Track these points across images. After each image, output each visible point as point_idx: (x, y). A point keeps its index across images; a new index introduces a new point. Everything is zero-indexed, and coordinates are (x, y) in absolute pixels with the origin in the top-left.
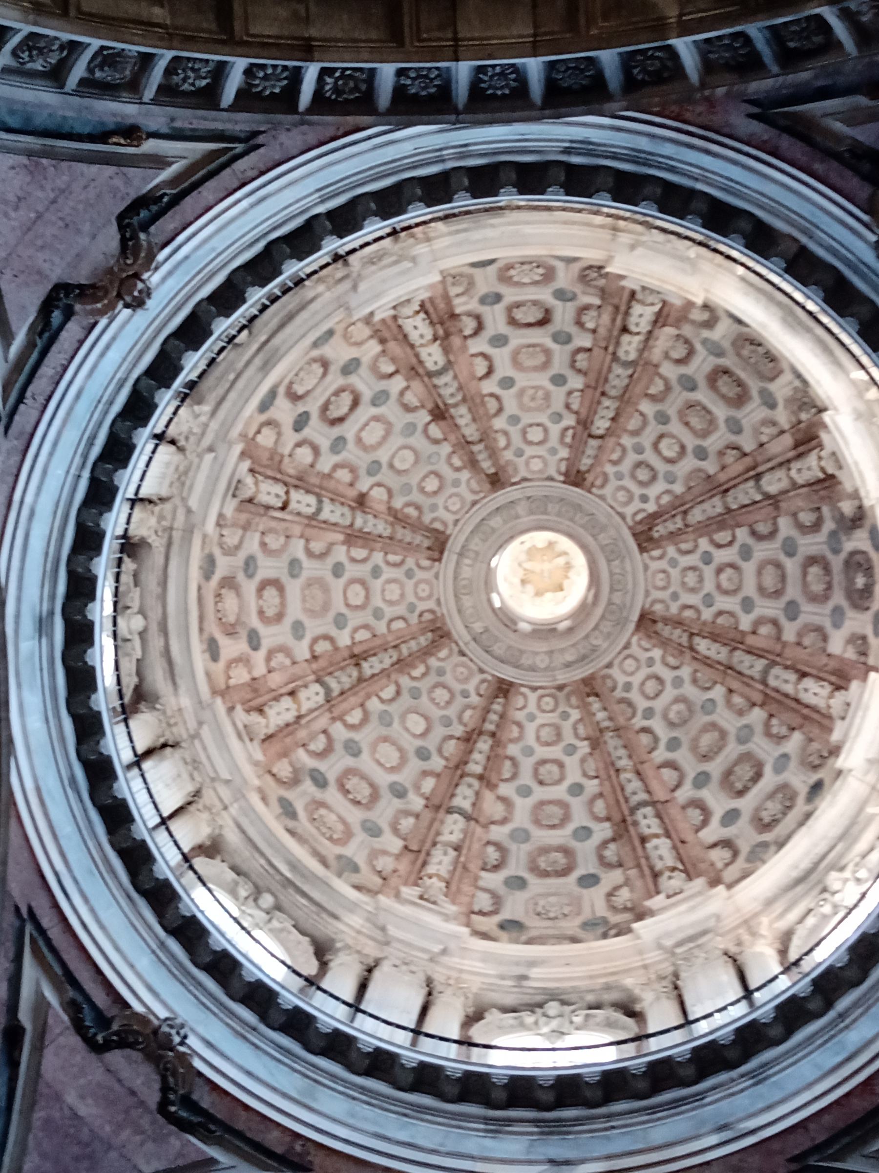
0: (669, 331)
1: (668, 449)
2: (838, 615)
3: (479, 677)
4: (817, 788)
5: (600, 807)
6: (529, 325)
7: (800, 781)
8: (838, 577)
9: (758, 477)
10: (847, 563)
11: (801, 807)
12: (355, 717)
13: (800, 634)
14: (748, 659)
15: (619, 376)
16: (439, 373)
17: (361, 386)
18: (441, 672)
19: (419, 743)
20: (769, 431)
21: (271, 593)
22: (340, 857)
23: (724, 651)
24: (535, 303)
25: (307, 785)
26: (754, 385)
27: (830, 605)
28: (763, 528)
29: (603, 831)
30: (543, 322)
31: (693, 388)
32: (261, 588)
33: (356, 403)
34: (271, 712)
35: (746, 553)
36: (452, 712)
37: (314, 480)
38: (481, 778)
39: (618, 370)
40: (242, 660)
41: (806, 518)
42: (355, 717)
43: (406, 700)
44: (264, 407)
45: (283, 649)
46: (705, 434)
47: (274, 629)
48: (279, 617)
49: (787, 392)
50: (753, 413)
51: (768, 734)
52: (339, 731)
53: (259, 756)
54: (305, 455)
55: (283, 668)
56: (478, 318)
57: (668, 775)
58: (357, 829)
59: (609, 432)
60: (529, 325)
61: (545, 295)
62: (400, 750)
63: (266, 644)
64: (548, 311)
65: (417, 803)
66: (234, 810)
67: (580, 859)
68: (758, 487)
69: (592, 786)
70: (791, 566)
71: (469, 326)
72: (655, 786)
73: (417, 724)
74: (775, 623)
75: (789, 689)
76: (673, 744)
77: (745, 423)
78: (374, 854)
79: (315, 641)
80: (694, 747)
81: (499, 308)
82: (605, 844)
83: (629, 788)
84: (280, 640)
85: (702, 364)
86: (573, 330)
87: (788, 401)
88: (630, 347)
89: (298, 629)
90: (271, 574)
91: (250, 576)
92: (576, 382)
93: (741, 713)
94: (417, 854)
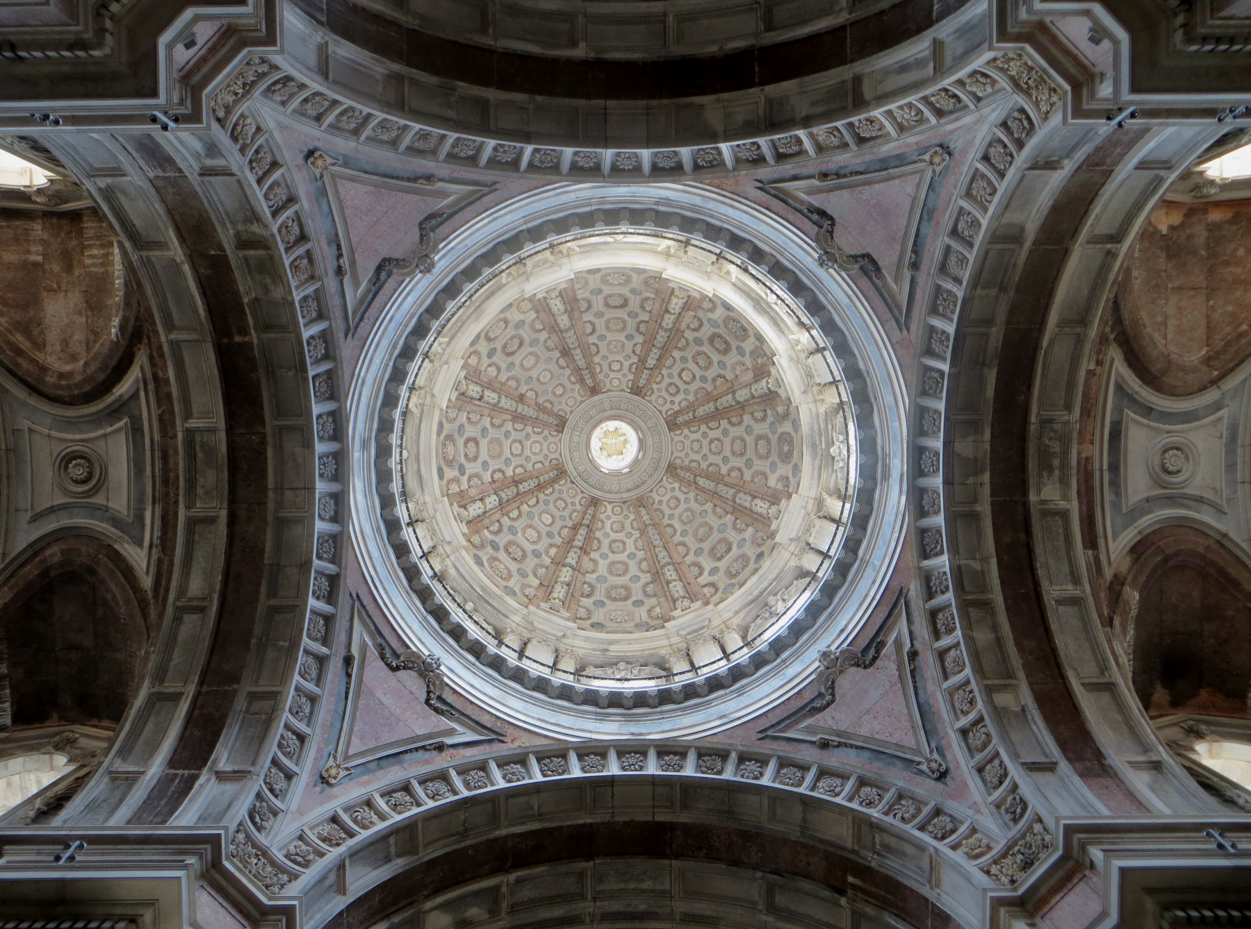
0: (692, 313)
1: (686, 376)
2: (773, 467)
3: (580, 495)
4: (760, 556)
5: (644, 564)
6: (616, 307)
7: (751, 552)
8: (774, 446)
9: (734, 393)
10: (779, 438)
11: (752, 566)
12: (514, 514)
13: (753, 477)
14: (725, 489)
15: (662, 337)
16: (567, 331)
17: (525, 336)
18: (560, 492)
19: (548, 529)
20: (739, 369)
21: (471, 444)
22: (506, 587)
23: (713, 484)
24: (619, 295)
25: (489, 548)
26: (734, 344)
27: (770, 461)
28: (734, 420)
29: (646, 578)
30: (622, 306)
31: (702, 345)
32: (466, 443)
33: (521, 344)
34: (471, 509)
35: (725, 433)
36: (566, 513)
37: (497, 385)
38: (581, 548)
39: (662, 333)
40: (456, 480)
41: (759, 415)
42: (514, 514)
43: (541, 506)
44: (473, 344)
45: (477, 475)
46: (706, 369)
47: (472, 465)
48: (475, 458)
49: (752, 347)
50: (732, 358)
51: (735, 528)
52: (505, 520)
53: (466, 531)
54: (492, 371)
55: (477, 486)
56: (589, 302)
57: (680, 548)
58: (514, 573)
59: (656, 367)
60: (616, 307)
61: (625, 291)
62: (538, 532)
63: (468, 472)
64: (626, 300)
65: (548, 561)
66: (452, 558)
67: (634, 593)
68: (734, 398)
69: (640, 555)
70: (750, 440)
71: (584, 305)
72: (674, 555)
73: (547, 519)
74: (740, 470)
75: (747, 504)
76: (684, 533)
77: (728, 364)
78: (524, 586)
79: (494, 472)
80: (695, 536)
81: (600, 297)
82: (647, 584)
83: (660, 556)
84: (476, 471)
85: (706, 332)
86: (639, 311)
87: (752, 353)
88: (668, 321)
89: (485, 464)
90: (472, 435)
91: (461, 436)
92: (639, 339)
93: (720, 517)
94: (547, 588)
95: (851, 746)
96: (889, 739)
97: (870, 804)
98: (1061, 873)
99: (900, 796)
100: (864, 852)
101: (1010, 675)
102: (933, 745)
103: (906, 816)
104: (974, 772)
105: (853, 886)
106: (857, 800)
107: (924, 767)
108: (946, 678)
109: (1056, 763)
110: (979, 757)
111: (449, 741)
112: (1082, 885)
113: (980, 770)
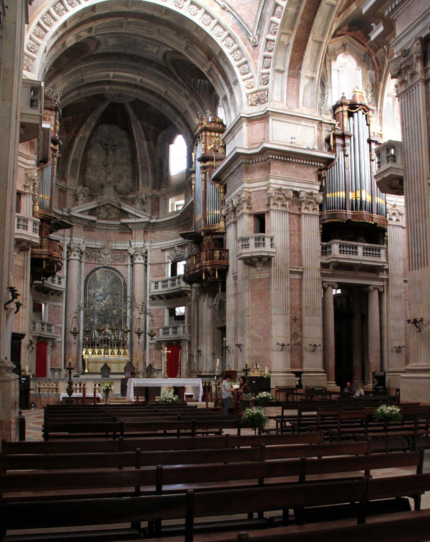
95: (232, 14)
96: (246, 21)
97: (228, 46)
98: (261, 117)
99: (238, 49)
100: (220, 58)
101: (292, 29)
102: (258, 32)
103: (237, 59)
104: (262, 57)
105: (214, 61)
106: (224, 43)
107: (251, 39)
108: (273, 15)
109: (284, 71)
110: (267, 53)
112: (263, 124)
113: (265, 57)
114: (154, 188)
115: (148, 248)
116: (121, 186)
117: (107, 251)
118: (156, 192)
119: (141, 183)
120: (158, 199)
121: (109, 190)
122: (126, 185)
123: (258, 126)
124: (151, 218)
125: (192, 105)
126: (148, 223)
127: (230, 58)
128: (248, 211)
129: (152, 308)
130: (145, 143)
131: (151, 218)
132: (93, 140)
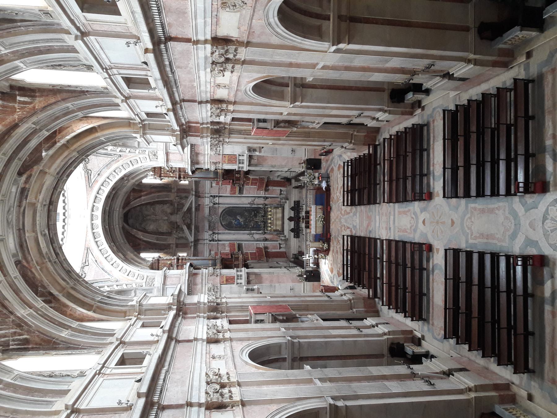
111: (94, 260)
114: (170, 191)
115: (209, 195)
116: (169, 211)
117: (210, 218)
118: (173, 191)
119: (167, 199)
120: (179, 189)
121: (173, 218)
122: (169, 207)
123: (171, 157)
124: (193, 195)
125: (133, 178)
126: (196, 196)
127: (128, 170)
128: (221, 164)
129: (244, 193)
130: (143, 198)
131: (193, 195)
132: (141, 229)
